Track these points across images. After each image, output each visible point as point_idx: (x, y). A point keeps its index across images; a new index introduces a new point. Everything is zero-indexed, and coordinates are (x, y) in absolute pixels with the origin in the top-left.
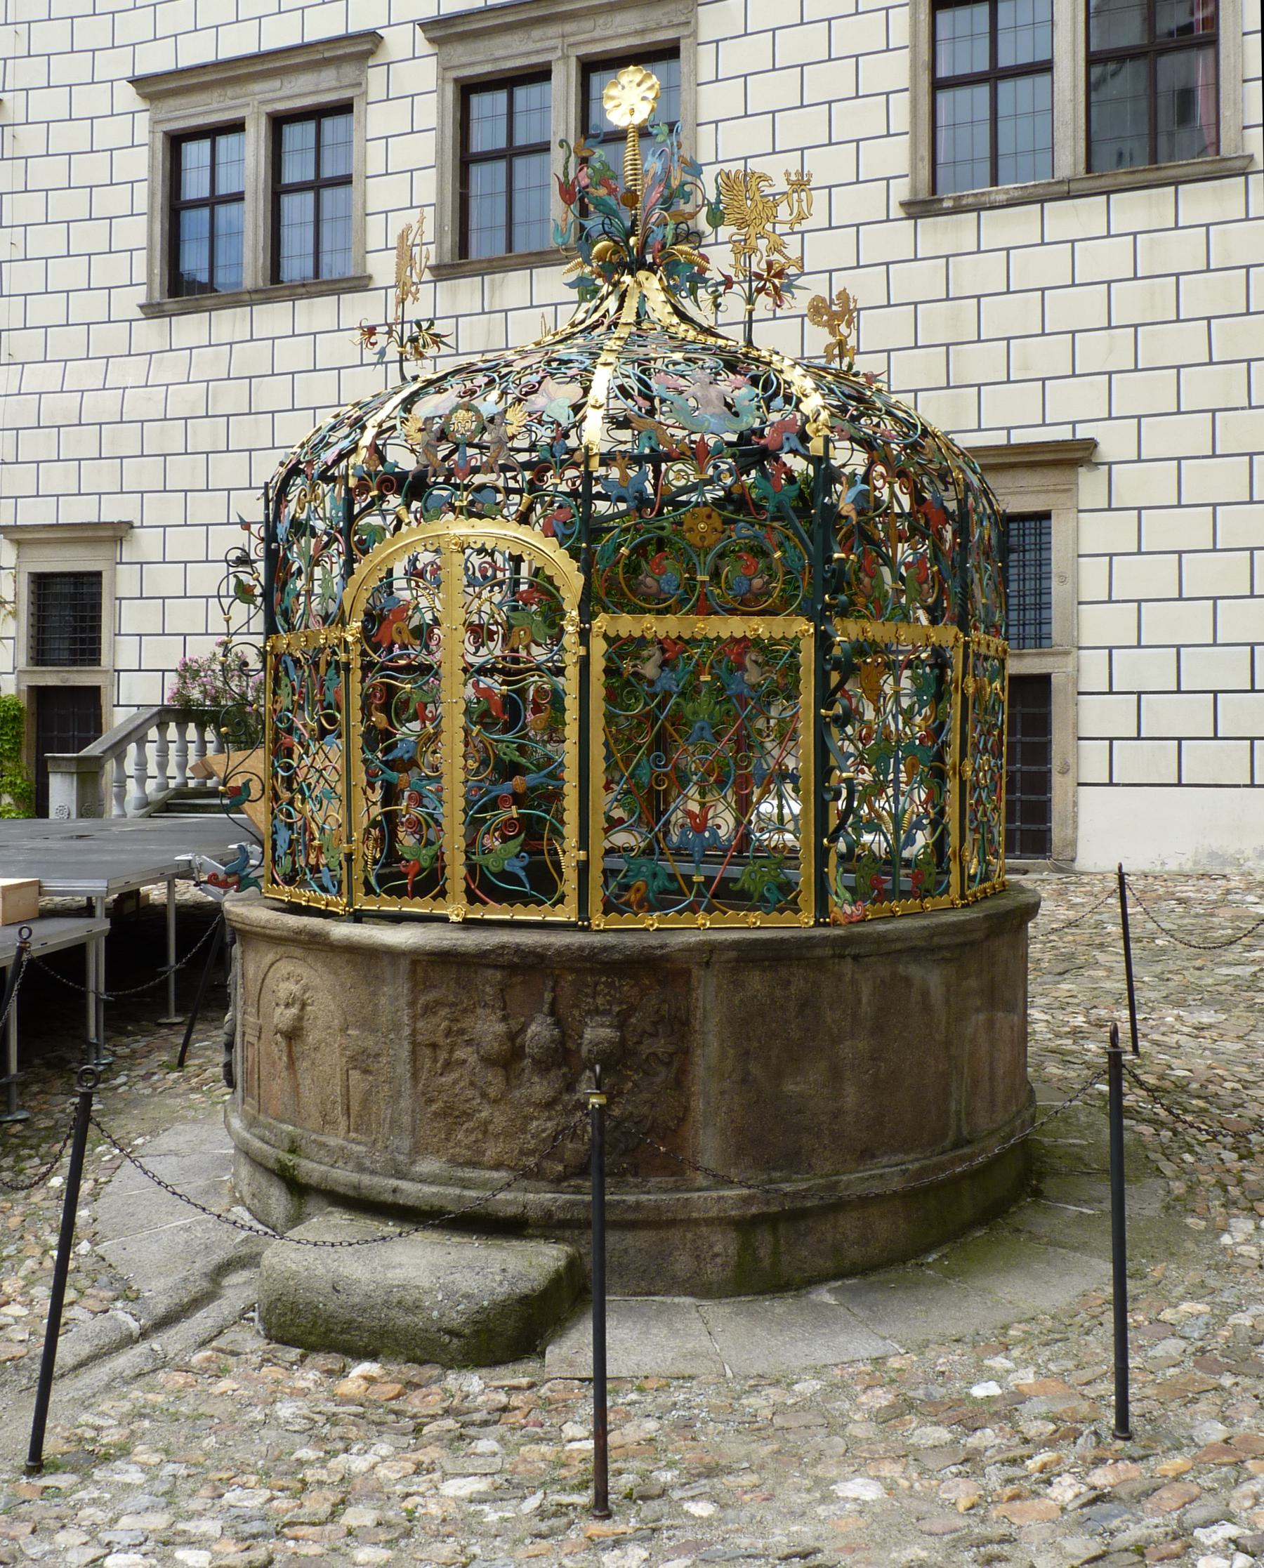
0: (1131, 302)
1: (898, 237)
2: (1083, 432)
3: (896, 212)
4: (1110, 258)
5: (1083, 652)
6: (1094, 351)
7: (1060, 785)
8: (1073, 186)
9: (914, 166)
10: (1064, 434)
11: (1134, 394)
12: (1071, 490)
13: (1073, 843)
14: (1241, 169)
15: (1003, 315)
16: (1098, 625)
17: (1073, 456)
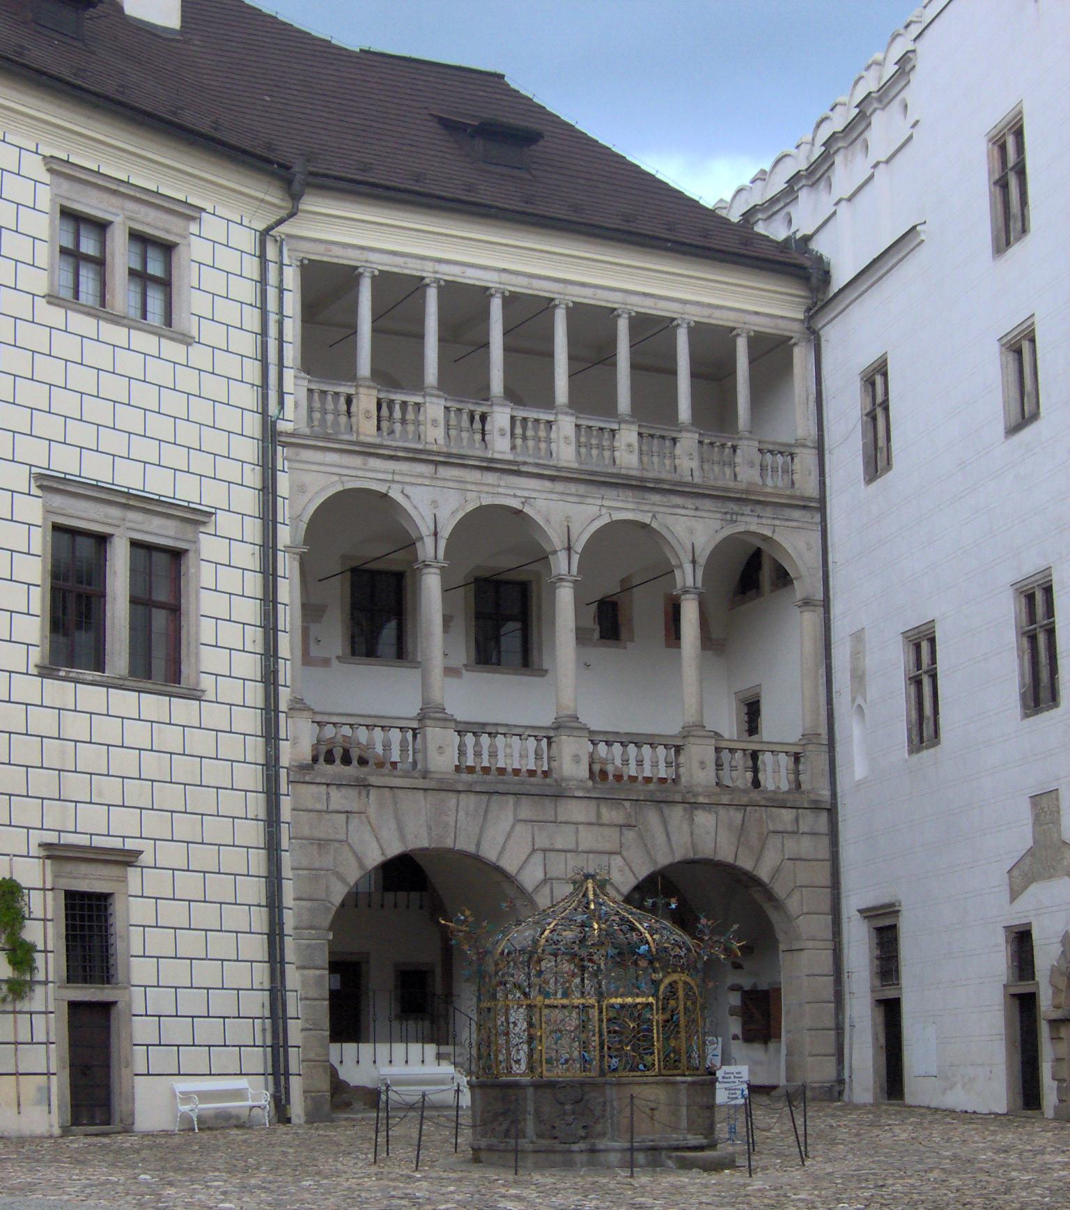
0: (153, 765)
1: (28, 688)
2: (130, 845)
3: (33, 670)
4: (138, 734)
5: (133, 989)
6: (137, 793)
7: (120, 1075)
8: (126, 683)
9: (42, 641)
10: (116, 843)
11: (155, 824)
12: (124, 880)
13: (132, 1114)
14: (195, 695)
15: (90, 757)
16: (140, 971)
17: (126, 859)
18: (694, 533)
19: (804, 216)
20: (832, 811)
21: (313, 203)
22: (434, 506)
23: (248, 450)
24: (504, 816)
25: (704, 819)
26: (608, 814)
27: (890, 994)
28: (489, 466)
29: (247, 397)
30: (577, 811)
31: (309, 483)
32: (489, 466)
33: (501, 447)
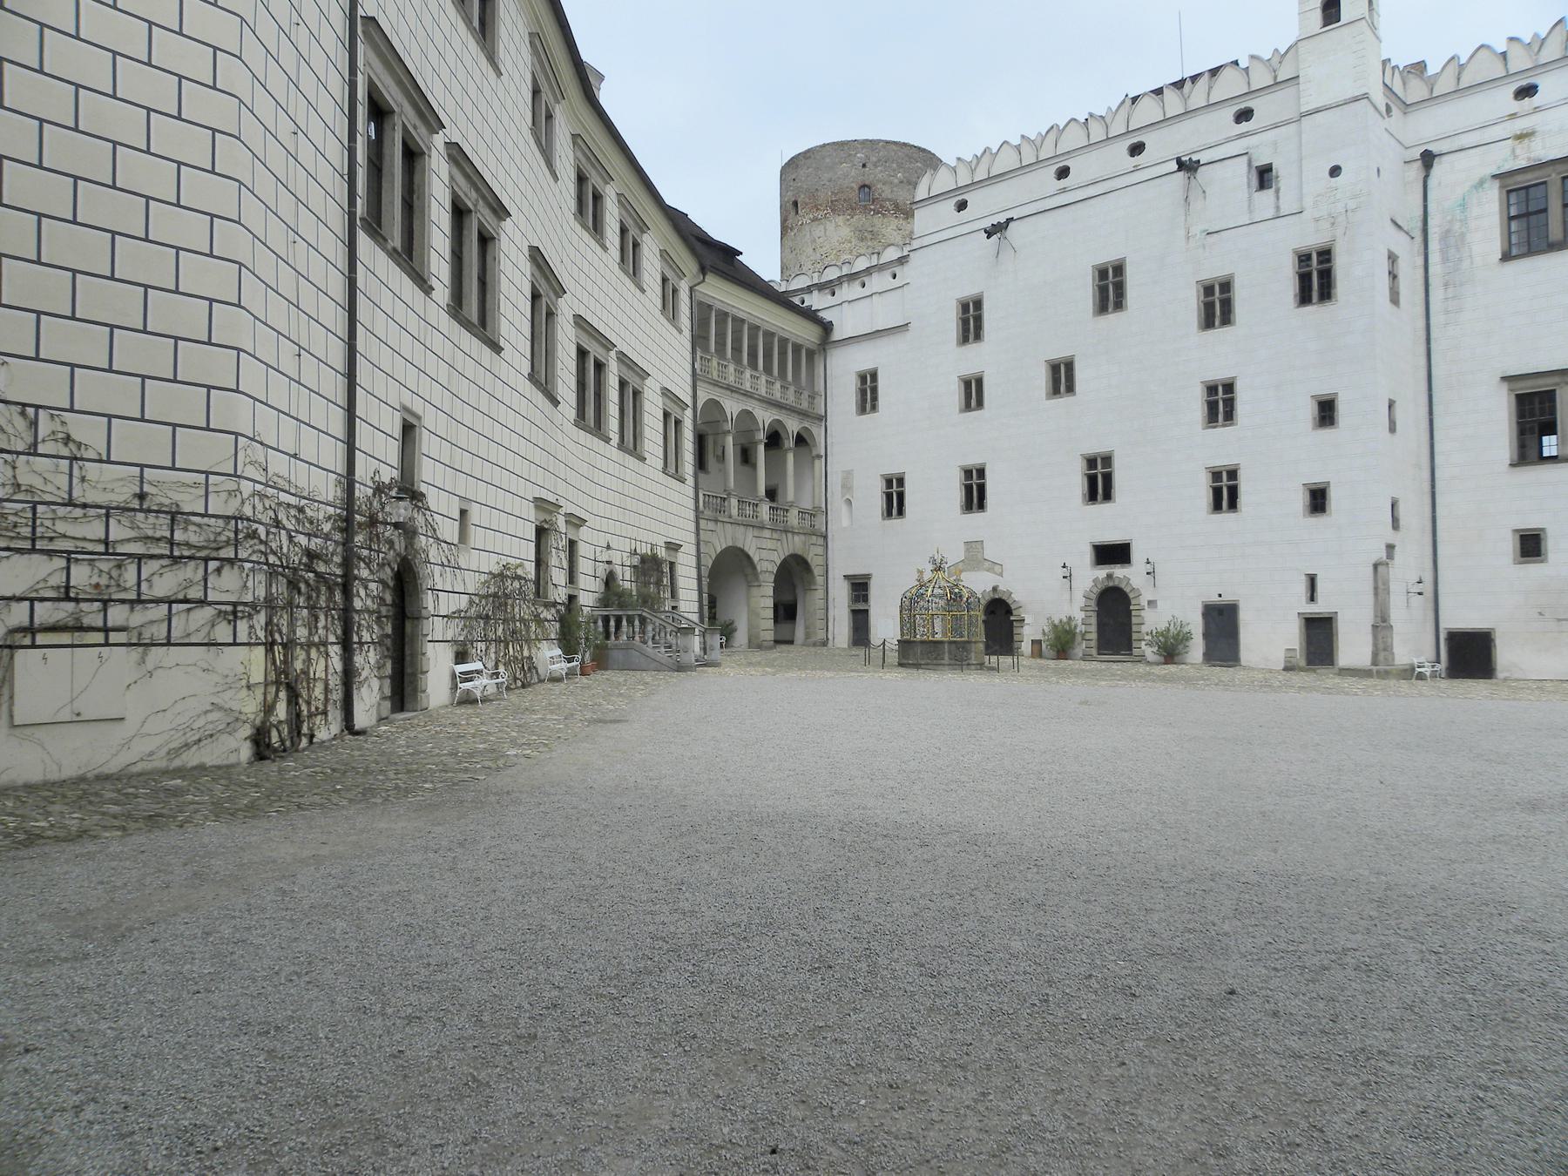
18: (793, 426)
19: (815, 301)
20: (825, 537)
21: (710, 278)
22: (732, 406)
23: (689, 379)
24: (750, 532)
25: (796, 538)
26: (775, 536)
27: (861, 606)
28: (746, 394)
29: (689, 357)
30: (767, 533)
31: (703, 397)
32: (746, 394)
33: (747, 386)
